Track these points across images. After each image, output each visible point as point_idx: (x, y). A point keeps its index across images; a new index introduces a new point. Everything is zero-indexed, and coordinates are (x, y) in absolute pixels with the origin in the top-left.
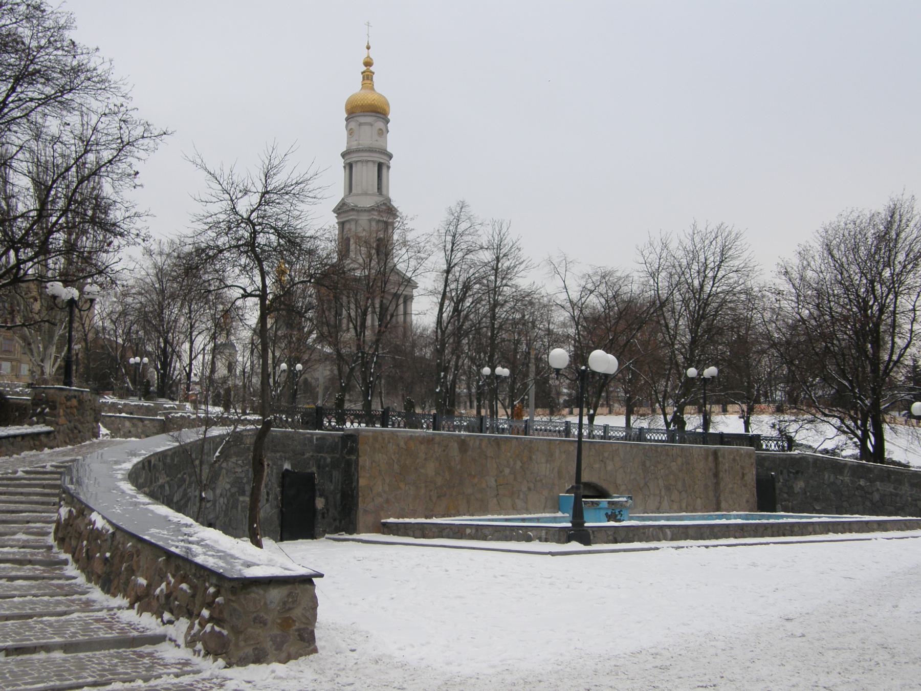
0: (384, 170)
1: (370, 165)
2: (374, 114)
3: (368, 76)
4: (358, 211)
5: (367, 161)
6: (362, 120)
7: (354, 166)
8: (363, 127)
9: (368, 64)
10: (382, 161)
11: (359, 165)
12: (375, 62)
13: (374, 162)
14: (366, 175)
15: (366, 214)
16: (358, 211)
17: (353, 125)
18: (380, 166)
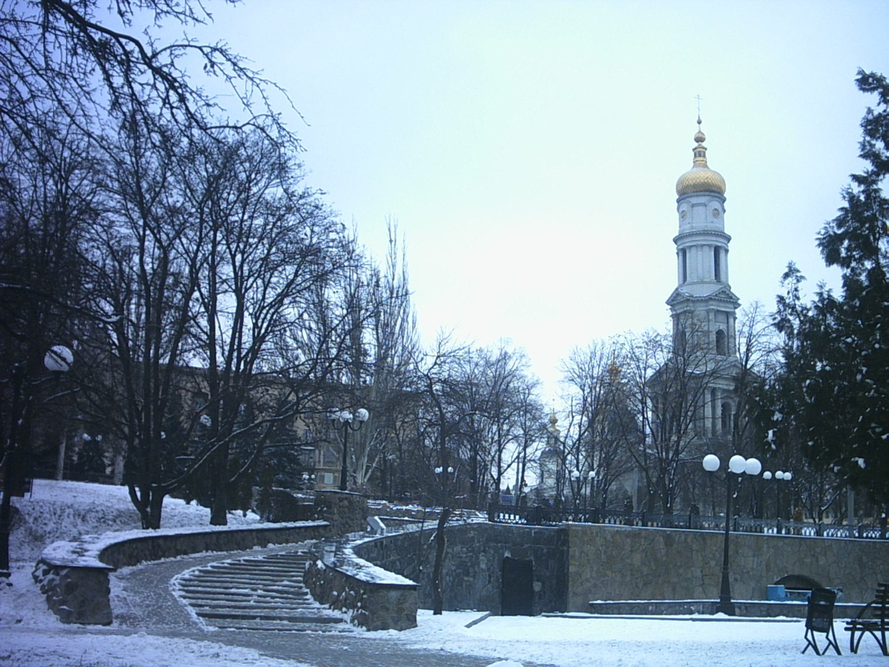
0: (722, 254)
1: (706, 249)
2: (707, 193)
3: (699, 154)
4: (693, 302)
5: (702, 246)
6: (694, 200)
7: (687, 251)
8: (696, 208)
9: (699, 139)
10: (719, 244)
11: (693, 250)
12: (706, 137)
13: (709, 246)
14: (702, 261)
15: (703, 304)
16: (693, 302)
17: (685, 207)
18: (717, 250)
